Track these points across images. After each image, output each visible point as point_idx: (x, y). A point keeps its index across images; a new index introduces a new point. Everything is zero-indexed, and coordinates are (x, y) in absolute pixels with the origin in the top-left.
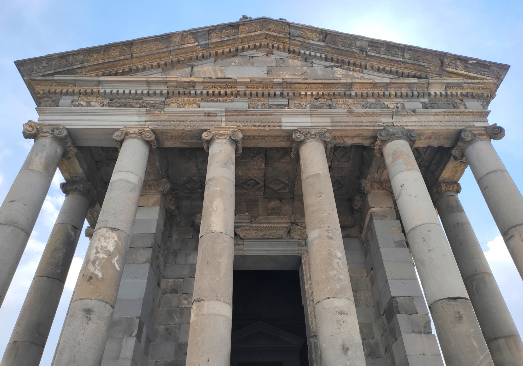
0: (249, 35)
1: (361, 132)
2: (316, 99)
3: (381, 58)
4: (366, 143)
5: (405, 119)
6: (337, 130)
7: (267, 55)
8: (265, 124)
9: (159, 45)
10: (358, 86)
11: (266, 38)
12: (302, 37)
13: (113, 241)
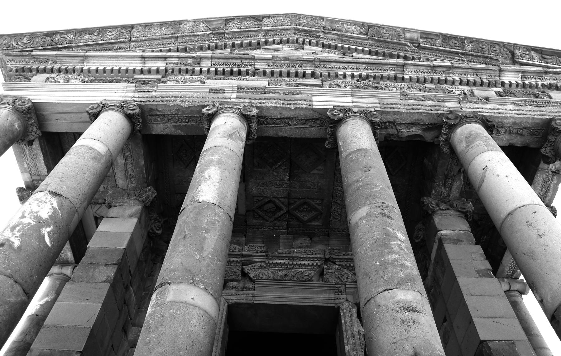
0: (275, 28)
1: (421, 117)
2: (357, 81)
3: (437, 50)
4: (429, 136)
5: (476, 106)
6: (388, 112)
7: (296, 49)
8: (290, 102)
9: (165, 31)
10: (413, 69)
11: (295, 34)
12: (338, 30)
13: (51, 206)
